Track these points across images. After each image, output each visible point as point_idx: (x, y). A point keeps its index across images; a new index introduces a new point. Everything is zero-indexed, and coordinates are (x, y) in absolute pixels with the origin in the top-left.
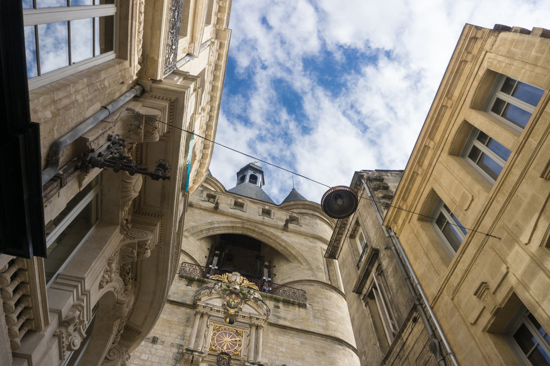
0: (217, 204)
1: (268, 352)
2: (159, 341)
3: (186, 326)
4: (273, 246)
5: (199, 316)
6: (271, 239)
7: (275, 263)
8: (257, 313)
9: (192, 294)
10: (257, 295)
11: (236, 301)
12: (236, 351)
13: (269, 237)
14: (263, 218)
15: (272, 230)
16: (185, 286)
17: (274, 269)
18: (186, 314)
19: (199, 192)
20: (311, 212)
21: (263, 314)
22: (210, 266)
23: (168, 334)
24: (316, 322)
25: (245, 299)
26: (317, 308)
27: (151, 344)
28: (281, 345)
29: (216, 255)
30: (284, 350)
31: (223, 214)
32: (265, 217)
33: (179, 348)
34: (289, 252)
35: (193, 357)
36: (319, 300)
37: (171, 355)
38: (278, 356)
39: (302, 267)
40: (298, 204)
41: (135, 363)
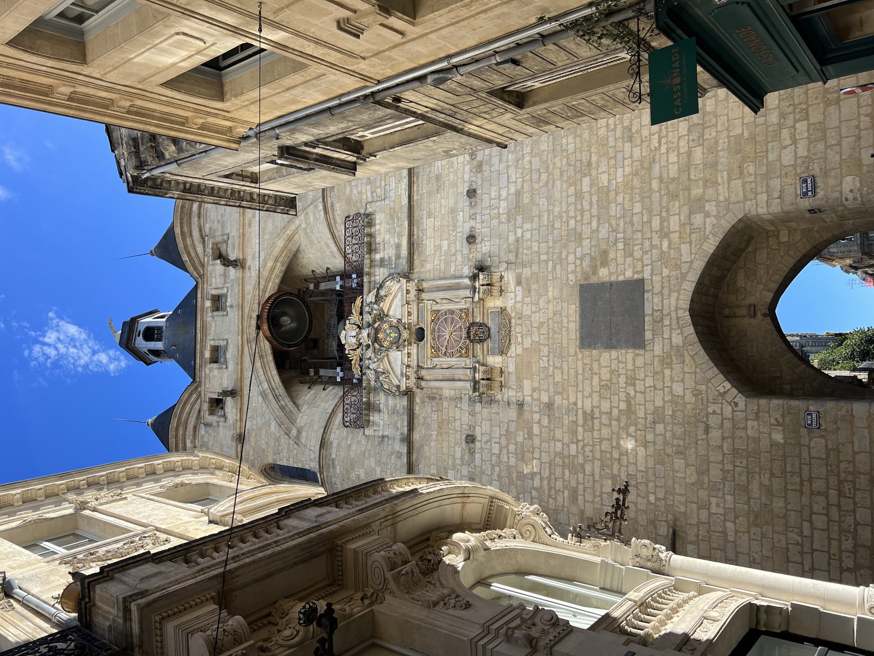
0: (226, 393)
1: (453, 269)
2: (470, 433)
3: (441, 399)
4: (278, 281)
5: (423, 384)
7: (307, 271)
8: (400, 294)
9: (391, 401)
10: (370, 298)
11: (388, 332)
12: (461, 318)
14: (231, 306)
15: (249, 287)
16: (381, 414)
17: (318, 271)
18: (423, 402)
19: (210, 431)
20: (195, 220)
21: (399, 285)
22: (339, 380)
23: (458, 422)
24: (392, 194)
25: (382, 317)
26: (369, 194)
27: (477, 443)
28: (440, 247)
29: (317, 373)
30: (445, 243)
32: (228, 304)
34: (282, 251)
35: (483, 379)
36: (355, 192)
37: (485, 411)
38: (456, 251)
39: (304, 225)
40: (186, 246)
41: (506, 460)
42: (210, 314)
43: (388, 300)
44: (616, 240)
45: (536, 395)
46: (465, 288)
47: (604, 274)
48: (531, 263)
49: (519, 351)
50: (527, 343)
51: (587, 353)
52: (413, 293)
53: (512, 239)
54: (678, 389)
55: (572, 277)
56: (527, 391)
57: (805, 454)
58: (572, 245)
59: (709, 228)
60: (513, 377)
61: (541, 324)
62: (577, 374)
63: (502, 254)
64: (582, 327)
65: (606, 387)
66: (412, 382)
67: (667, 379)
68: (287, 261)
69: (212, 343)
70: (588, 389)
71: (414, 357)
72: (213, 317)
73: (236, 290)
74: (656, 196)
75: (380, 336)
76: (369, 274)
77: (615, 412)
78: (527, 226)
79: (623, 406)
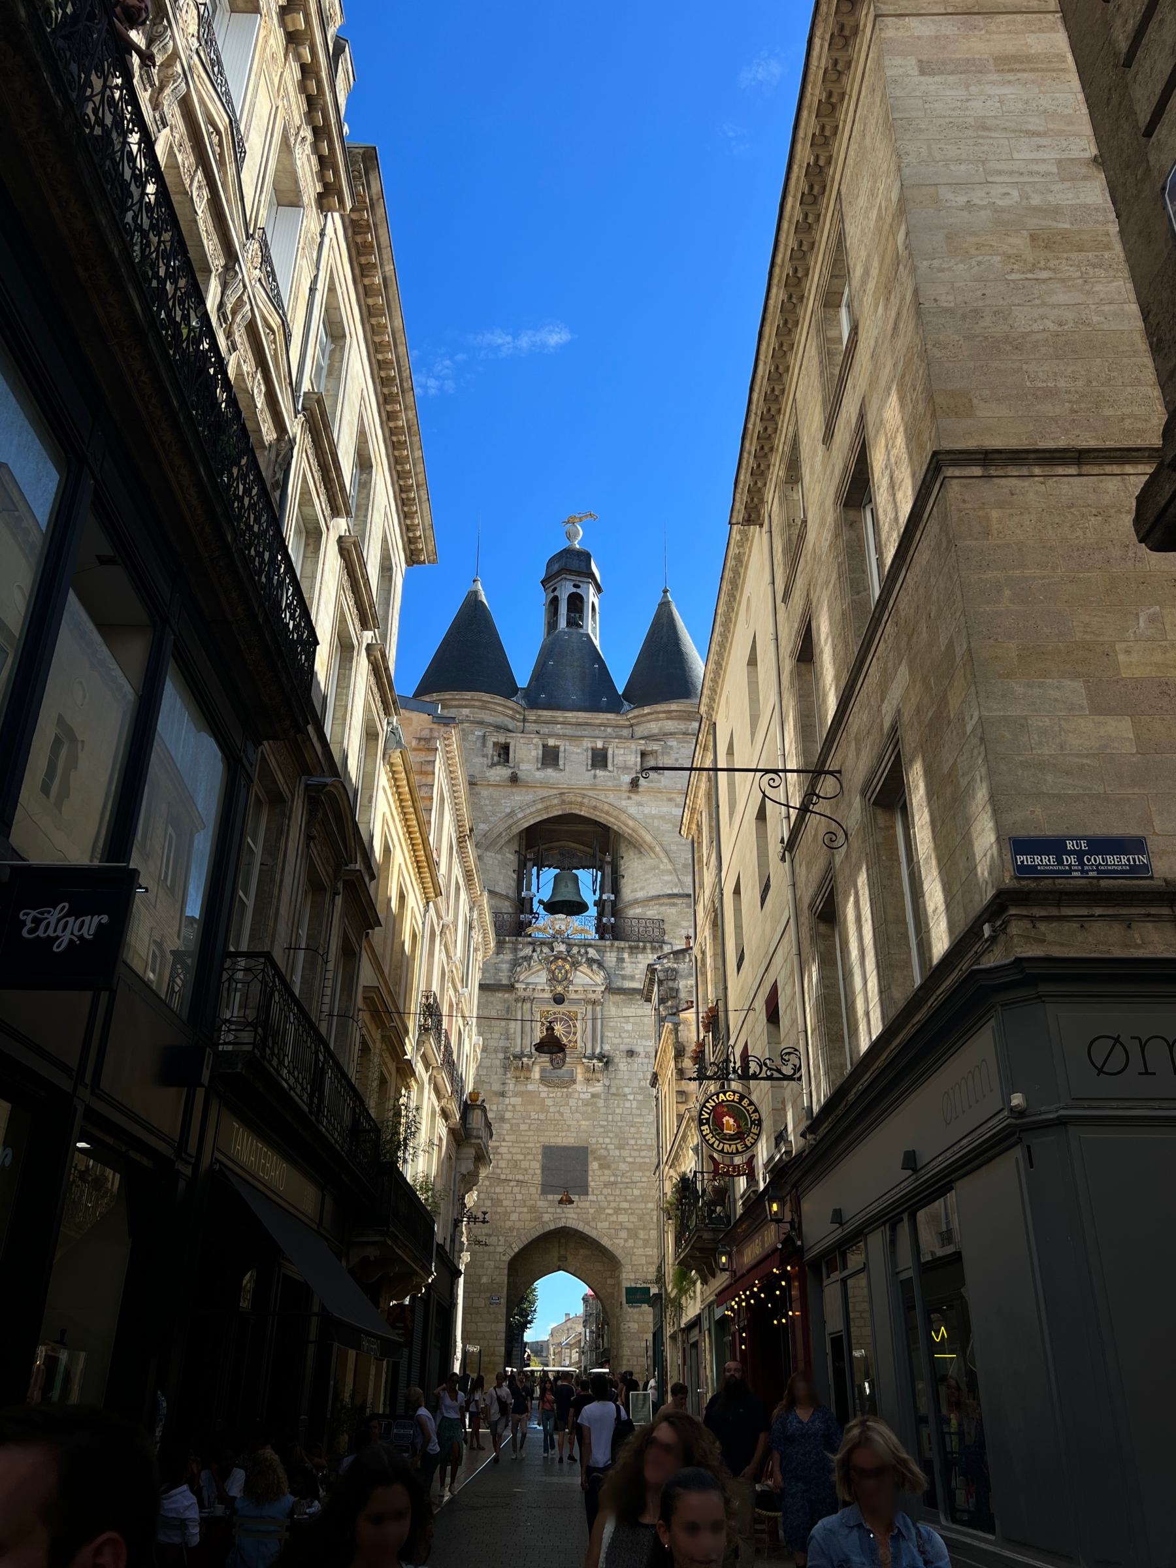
1: (609, 1034)
4: (615, 827)
6: (611, 816)
9: (505, 966)
13: (607, 813)
18: (505, 1001)
19: (479, 744)
25: (575, 965)
29: (530, 860)
31: (527, 785)
33: (506, 1052)
37: (498, 1062)
40: (658, 713)
42: (590, 745)
43: (588, 971)
44: (617, 1176)
45: (510, 1108)
46: (593, 1048)
47: (594, 1165)
48: (607, 1107)
49: (543, 1095)
50: (549, 1102)
51: (540, 1151)
52: (593, 996)
53: (627, 1090)
54: (514, 1217)
55: (594, 1141)
56: (514, 1100)
57: (475, 1295)
58: (616, 1141)
59: (617, 1241)
60: (523, 1088)
61: (562, 1114)
62: (525, 1143)
63: (617, 1081)
64: (559, 1148)
65: (515, 1165)
66: (521, 993)
67: (521, 1210)
68: (633, 841)
69: (562, 749)
70: (514, 1150)
71: (541, 995)
72: (586, 750)
73: (610, 783)
74: (642, 1206)
75: (560, 962)
76: (612, 945)
77: (499, 1171)
78: (635, 1104)
79: (503, 1177)
